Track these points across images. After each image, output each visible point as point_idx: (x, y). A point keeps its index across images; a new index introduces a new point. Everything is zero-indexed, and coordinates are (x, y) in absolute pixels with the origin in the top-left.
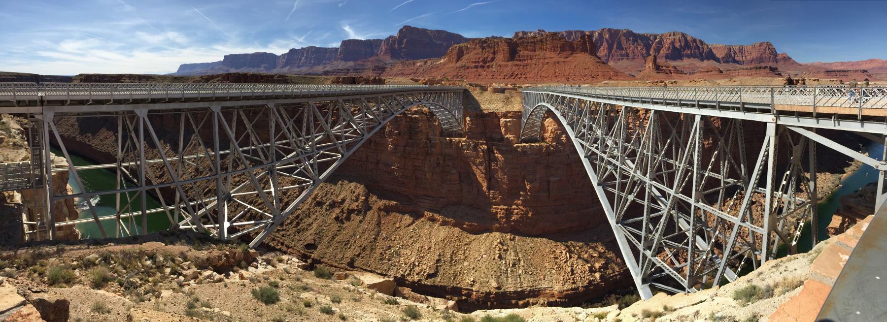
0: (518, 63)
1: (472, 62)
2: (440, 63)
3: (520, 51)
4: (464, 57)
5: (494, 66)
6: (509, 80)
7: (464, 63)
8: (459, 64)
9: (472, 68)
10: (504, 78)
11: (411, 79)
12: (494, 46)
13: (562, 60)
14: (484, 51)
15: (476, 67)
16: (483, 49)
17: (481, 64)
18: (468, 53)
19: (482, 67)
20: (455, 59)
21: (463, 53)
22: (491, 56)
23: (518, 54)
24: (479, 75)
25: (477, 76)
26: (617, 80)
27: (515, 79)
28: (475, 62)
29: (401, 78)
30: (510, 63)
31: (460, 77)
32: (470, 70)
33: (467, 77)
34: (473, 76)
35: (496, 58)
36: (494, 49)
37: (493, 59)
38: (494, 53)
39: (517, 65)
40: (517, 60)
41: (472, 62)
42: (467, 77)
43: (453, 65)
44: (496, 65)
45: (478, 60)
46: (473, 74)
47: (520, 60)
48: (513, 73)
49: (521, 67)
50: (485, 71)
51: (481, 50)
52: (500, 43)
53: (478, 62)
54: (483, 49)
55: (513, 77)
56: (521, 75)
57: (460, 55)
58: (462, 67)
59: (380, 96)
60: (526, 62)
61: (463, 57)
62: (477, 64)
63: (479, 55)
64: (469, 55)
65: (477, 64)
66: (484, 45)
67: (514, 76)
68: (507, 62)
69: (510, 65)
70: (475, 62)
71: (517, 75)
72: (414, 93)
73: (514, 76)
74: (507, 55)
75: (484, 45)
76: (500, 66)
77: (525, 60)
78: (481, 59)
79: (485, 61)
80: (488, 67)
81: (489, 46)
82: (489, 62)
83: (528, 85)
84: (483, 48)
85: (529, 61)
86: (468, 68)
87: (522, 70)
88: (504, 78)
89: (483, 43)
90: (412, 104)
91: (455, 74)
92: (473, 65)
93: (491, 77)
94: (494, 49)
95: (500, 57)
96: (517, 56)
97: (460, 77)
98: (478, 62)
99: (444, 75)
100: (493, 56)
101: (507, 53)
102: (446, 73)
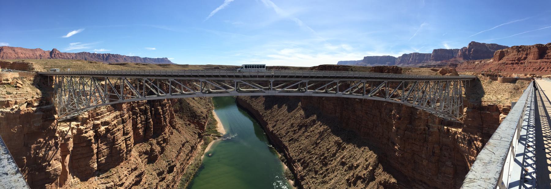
0: (547, 60)
1: (510, 61)
2: (490, 62)
3: (549, 53)
4: (505, 57)
5: (526, 63)
6: (537, 72)
7: (504, 61)
8: (501, 62)
9: (509, 64)
10: (533, 71)
12: (527, 50)
14: (519, 53)
15: (512, 64)
16: (518, 52)
17: (516, 61)
18: (508, 55)
19: (517, 63)
20: (498, 59)
21: (504, 55)
22: (524, 56)
23: (547, 55)
24: (514, 69)
25: (513, 70)
27: (541, 72)
28: (512, 61)
30: (539, 61)
31: (500, 70)
32: (508, 65)
33: (505, 70)
34: (509, 70)
35: (528, 58)
36: (527, 52)
37: (525, 58)
38: (527, 54)
39: (546, 62)
40: (546, 59)
41: (510, 61)
42: (505, 70)
43: (496, 62)
44: (527, 62)
45: (514, 59)
46: (510, 68)
47: (548, 59)
48: (540, 67)
49: (549, 63)
50: (519, 66)
51: (517, 53)
52: (531, 48)
53: (514, 61)
54: (518, 52)
55: (540, 70)
56: (548, 68)
57: (502, 56)
58: (503, 64)
61: (504, 58)
62: (513, 62)
65: (513, 62)
66: (520, 50)
67: (541, 69)
68: (537, 60)
69: (539, 63)
70: (512, 61)
71: (543, 69)
73: (541, 69)
74: (537, 55)
75: (520, 50)
76: (530, 62)
78: (516, 59)
79: (519, 60)
80: (522, 63)
81: (523, 50)
82: (522, 60)
84: (519, 51)
86: (507, 64)
87: (549, 65)
88: (533, 71)
89: (519, 49)
91: (497, 68)
92: (511, 62)
94: (527, 52)
95: (531, 57)
96: (546, 55)
97: (500, 70)
98: (514, 61)
99: (489, 69)
100: (526, 56)
101: (537, 54)
102: (491, 68)
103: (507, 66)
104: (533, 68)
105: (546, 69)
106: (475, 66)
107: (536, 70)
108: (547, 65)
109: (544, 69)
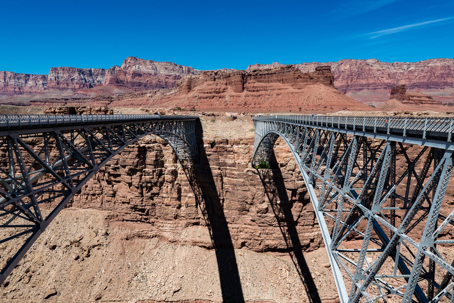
5: (227, 96)
8: (191, 94)
11: (141, 110)
13: (297, 90)
26: (353, 110)
29: (131, 109)
41: (204, 93)
43: (184, 95)
45: (210, 91)
53: (210, 93)
59: (108, 126)
60: (260, 93)
62: (209, 95)
63: (211, 87)
64: (201, 86)
65: (209, 95)
68: (240, 92)
70: (208, 93)
72: (145, 123)
77: (258, 91)
78: (213, 90)
83: (260, 114)
85: (263, 92)
90: (144, 133)
93: (223, 107)
97: (192, 107)
98: (210, 93)
103: (200, 100)
104: (237, 104)
105: (253, 105)
106: (147, 100)
107: (241, 107)
108: (254, 100)
109: (251, 106)
